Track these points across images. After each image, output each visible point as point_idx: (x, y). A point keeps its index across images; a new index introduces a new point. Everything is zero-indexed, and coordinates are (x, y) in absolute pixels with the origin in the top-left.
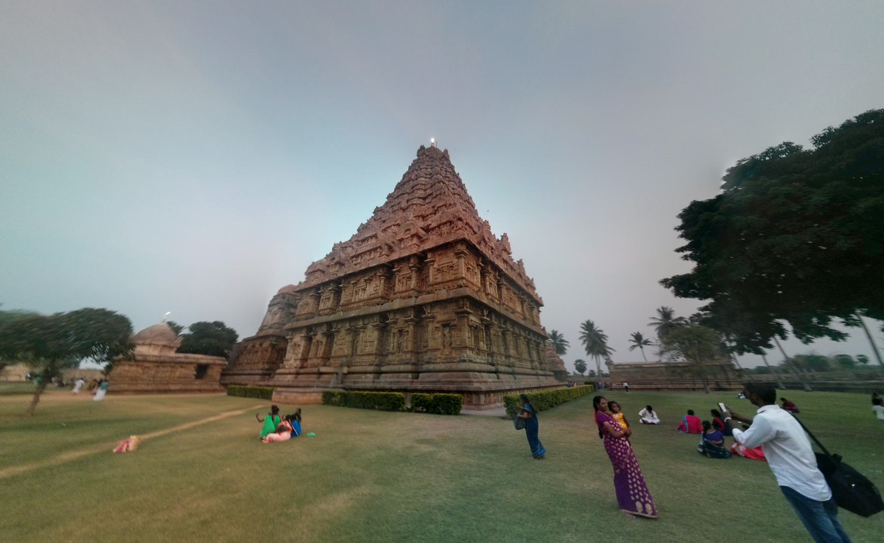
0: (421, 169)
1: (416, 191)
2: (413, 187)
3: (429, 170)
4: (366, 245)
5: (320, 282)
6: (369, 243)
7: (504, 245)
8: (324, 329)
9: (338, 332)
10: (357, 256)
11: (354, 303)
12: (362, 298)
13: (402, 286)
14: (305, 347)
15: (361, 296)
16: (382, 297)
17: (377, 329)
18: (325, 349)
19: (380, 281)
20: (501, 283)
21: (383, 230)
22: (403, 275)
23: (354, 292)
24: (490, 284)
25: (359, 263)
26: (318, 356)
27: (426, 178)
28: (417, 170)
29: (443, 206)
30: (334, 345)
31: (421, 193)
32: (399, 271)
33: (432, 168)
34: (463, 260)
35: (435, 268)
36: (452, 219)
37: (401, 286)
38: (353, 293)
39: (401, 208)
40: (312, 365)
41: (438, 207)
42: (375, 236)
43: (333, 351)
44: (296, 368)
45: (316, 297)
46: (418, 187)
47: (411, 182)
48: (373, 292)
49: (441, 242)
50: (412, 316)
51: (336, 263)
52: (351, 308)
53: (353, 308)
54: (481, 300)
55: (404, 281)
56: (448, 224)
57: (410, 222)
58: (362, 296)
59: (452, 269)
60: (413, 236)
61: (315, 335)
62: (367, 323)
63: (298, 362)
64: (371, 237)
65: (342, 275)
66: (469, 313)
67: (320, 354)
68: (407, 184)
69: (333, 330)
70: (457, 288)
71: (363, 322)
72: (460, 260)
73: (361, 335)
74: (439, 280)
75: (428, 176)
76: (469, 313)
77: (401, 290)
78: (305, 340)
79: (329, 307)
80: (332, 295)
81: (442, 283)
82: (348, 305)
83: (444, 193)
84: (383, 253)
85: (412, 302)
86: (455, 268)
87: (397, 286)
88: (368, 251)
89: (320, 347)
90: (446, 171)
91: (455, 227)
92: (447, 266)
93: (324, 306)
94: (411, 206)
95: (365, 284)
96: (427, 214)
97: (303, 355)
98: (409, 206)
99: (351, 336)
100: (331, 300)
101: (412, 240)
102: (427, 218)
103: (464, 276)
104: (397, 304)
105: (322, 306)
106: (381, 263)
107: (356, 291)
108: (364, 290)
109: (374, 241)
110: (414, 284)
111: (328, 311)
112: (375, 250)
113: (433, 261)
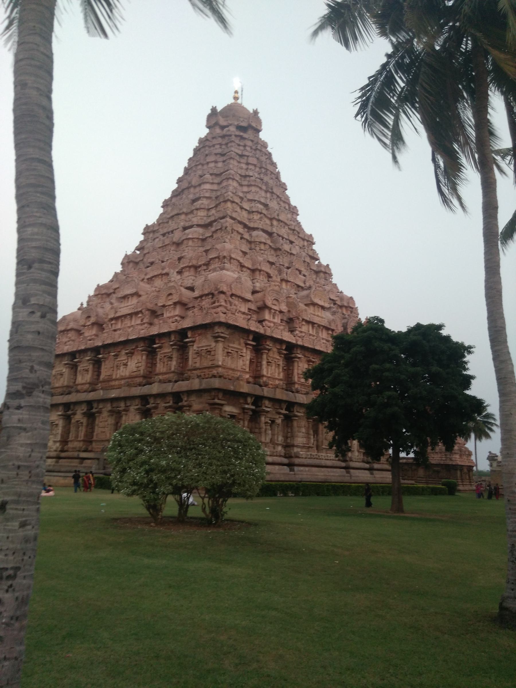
0: (208, 163)
1: (195, 212)
2: (194, 201)
3: (220, 165)
4: (126, 305)
5: (75, 349)
6: (129, 304)
7: (311, 298)
8: (84, 408)
9: (100, 412)
10: (117, 319)
11: (116, 380)
12: (123, 374)
13: (164, 367)
14: (64, 427)
15: (123, 371)
16: (144, 377)
17: (138, 413)
18: (86, 431)
19: (142, 357)
20: (293, 355)
21: (148, 279)
22: (165, 353)
23: (115, 366)
24: (268, 362)
25: (120, 329)
26: (79, 439)
27: (212, 183)
28: (203, 165)
29: (215, 258)
30: (96, 428)
31: (200, 217)
32: (160, 347)
33: (224, 162)
34: (220, 346)
35: (195, 350)
36: (213, 291)
37: (162, 366)
38: (113, 367)
39: (174, 243)
40: (73, 448)
41: (211, 259)
42: (137, 294)
43: (95, 434)
44: (56, 451)
45: (71, 366)
46: (197, 204)
47: (192, 190)
48: (135, 369)
49: (200, 321)
50: (171, 402)
51: (93, 324)
52: (112, 386)
53: (114, 385)
54: (237, 390)
55: (166, 360)
56: (210, 296)
57: (172, 284)
58: (123, 372)
59: (210, 354)
60: (175, 304)
61: (74, 414)
62: (129, 405)
63: (58, 444)
64: (132, 295)
65: (100, 344)
66: (222, 405)
67: (81, 437)
68: (186, 192)
69: (94, 410)
70: (211, 378)
71: (125, 404)
72: (218, 344)
73: (124, 418)
74: (198, 365)
75: (217, 180)
76: (222, 405)
77: (161, 371)
78: (64, 419)
79: (88, 381)
80: (91, 367)
81: (200, 369)
82: (109, 381)
83: (226, 227)
84: (144, 321)
85: (169, 388)
86: (212, 353)
87: (158, 365)
88: (129, 314)
89: (80, 429)
90: (248, 164)
91: (216, 302)
92: (206, 349)
93: (82, 379)
94: (185, 242)
95: (125, 358)
96: (200, 263)
97: (62, 436)
98: (183, 240)
99: (114, 417)
100: (90, 372)
101: (175, 308)
102: (200, 269)
103: (220, 363)
104: (155, 389)
105: (80, 379)
106: (141, 336)
107: (117, 366)
108: (126, 365)
109: (134, 301)
110: (175, 366)
111: (87, 386)
112: (136, 313)
113: (193, 342)
